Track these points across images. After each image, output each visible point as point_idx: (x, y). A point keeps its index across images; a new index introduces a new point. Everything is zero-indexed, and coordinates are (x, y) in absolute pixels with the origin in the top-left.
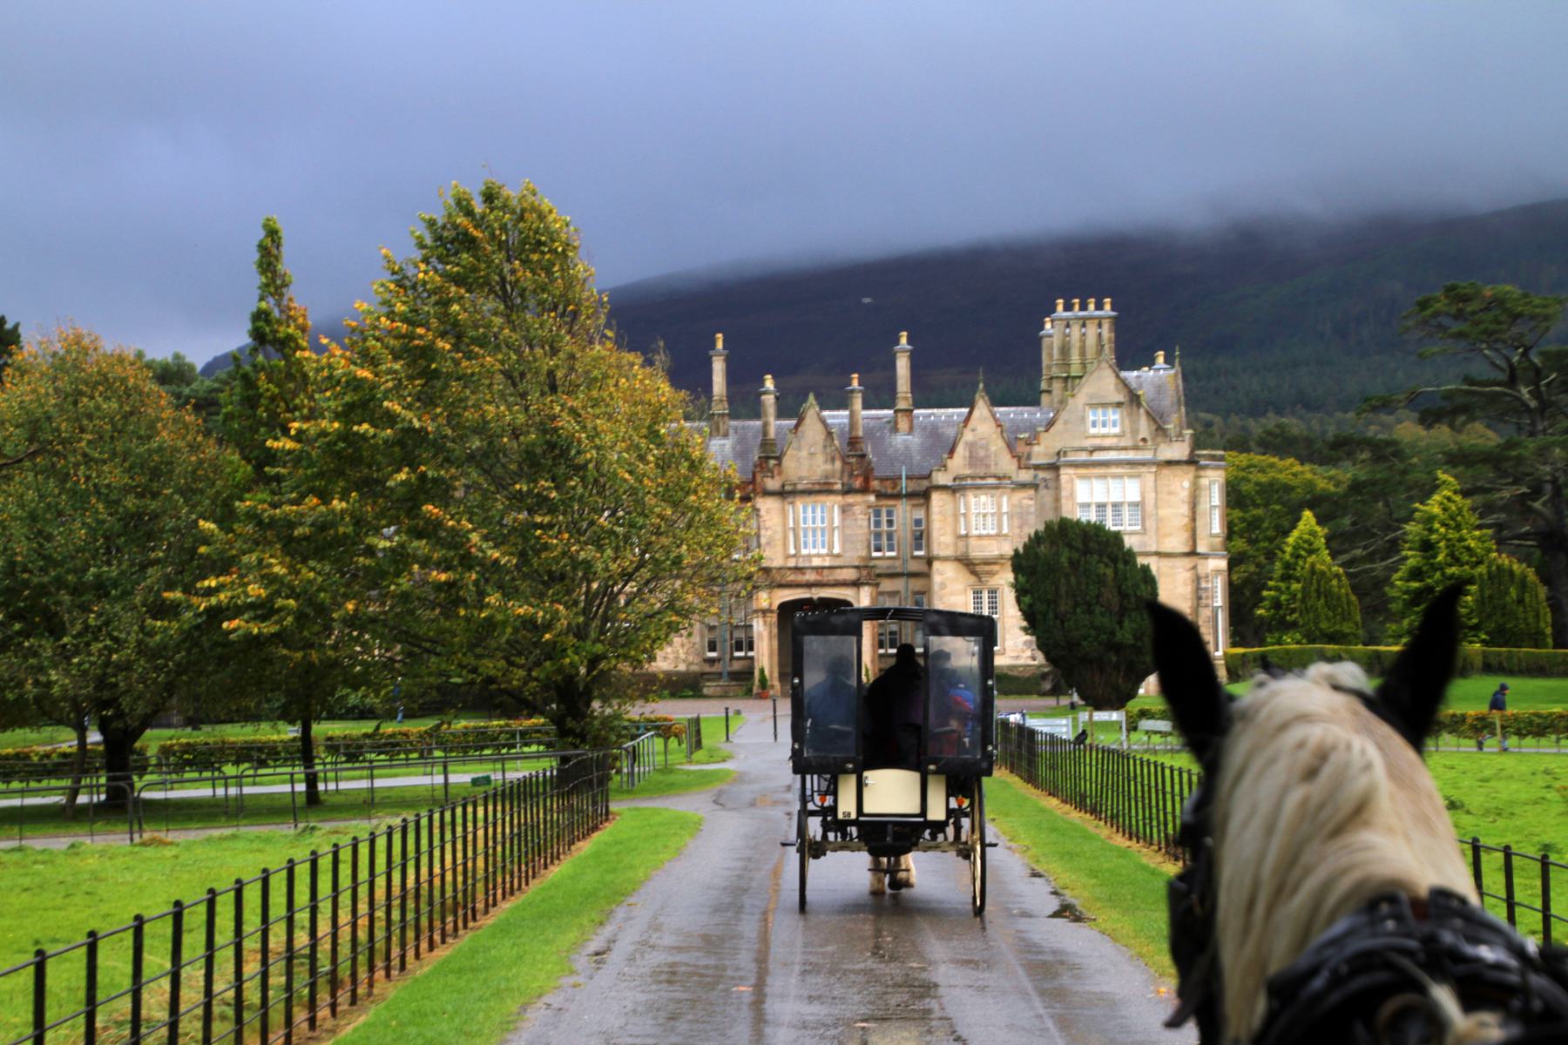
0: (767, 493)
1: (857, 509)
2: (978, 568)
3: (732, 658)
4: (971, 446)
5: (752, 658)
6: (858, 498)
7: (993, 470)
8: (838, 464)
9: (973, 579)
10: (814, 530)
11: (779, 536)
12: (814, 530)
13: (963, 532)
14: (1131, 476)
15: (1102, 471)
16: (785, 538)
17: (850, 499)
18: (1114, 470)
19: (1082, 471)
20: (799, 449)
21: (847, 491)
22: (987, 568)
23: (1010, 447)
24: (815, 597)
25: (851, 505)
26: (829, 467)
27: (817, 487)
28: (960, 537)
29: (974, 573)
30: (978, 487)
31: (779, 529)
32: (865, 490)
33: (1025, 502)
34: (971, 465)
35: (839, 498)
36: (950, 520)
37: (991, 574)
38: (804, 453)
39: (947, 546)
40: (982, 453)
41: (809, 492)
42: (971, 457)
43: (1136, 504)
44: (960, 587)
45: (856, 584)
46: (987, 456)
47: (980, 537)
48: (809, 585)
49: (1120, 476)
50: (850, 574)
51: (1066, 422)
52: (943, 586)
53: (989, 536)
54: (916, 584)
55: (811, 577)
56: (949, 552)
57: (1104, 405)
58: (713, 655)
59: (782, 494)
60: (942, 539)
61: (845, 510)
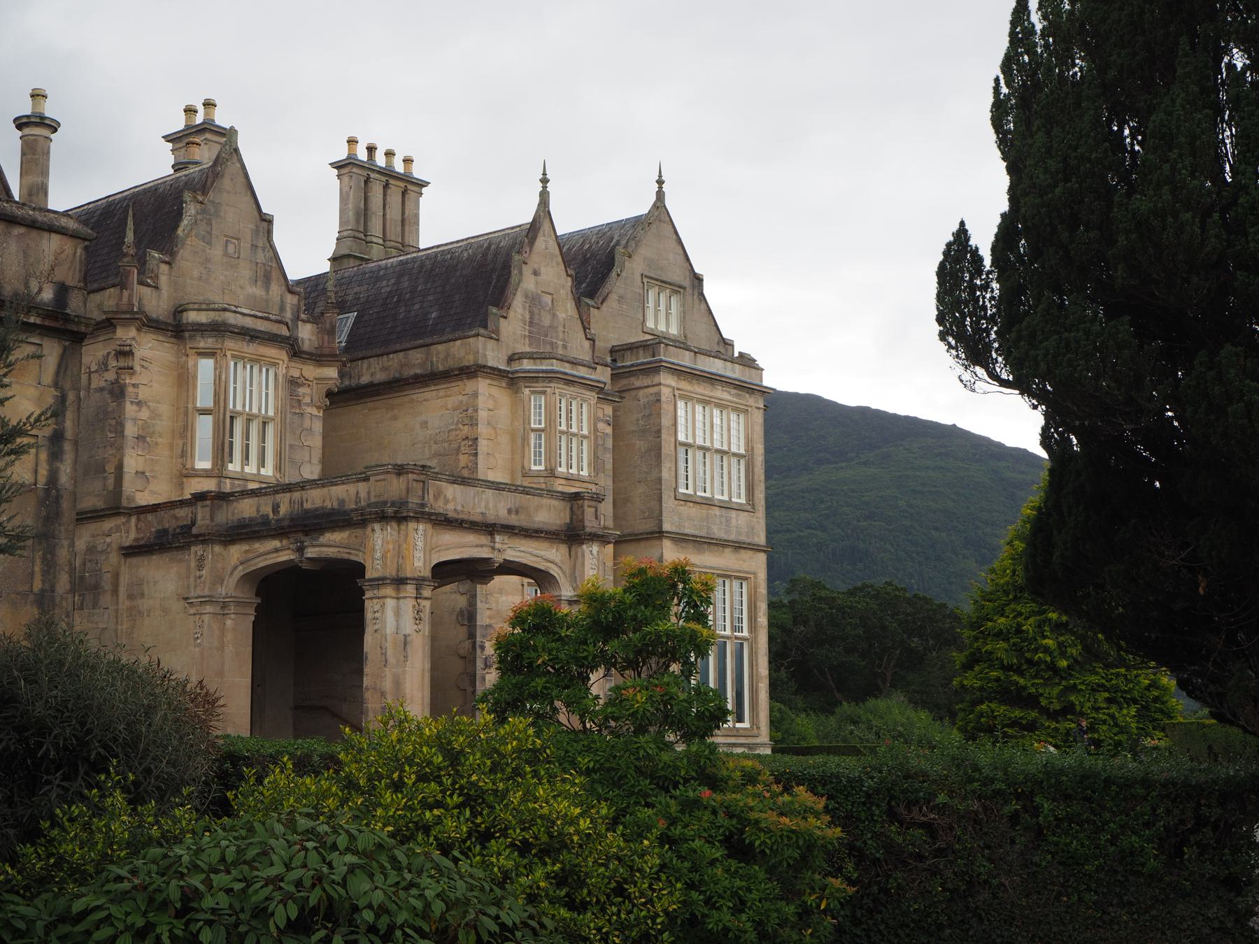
7: (560, 351)
8: (276, 289)
11: (164, 425)
15: (702, 389)
16: (185, 432)
18: (721, 393)
19: (684, 385)
20: (208, 240)
26: (258, 291)
27: (261, 326)
30: (569, 381)
31: (165, 409)
34: (531, 338)
38: (216, 252)
42: (531, 323)
46: (553, 327)
48: (489, 528)
49: (722, 406)
51: (621, 298)
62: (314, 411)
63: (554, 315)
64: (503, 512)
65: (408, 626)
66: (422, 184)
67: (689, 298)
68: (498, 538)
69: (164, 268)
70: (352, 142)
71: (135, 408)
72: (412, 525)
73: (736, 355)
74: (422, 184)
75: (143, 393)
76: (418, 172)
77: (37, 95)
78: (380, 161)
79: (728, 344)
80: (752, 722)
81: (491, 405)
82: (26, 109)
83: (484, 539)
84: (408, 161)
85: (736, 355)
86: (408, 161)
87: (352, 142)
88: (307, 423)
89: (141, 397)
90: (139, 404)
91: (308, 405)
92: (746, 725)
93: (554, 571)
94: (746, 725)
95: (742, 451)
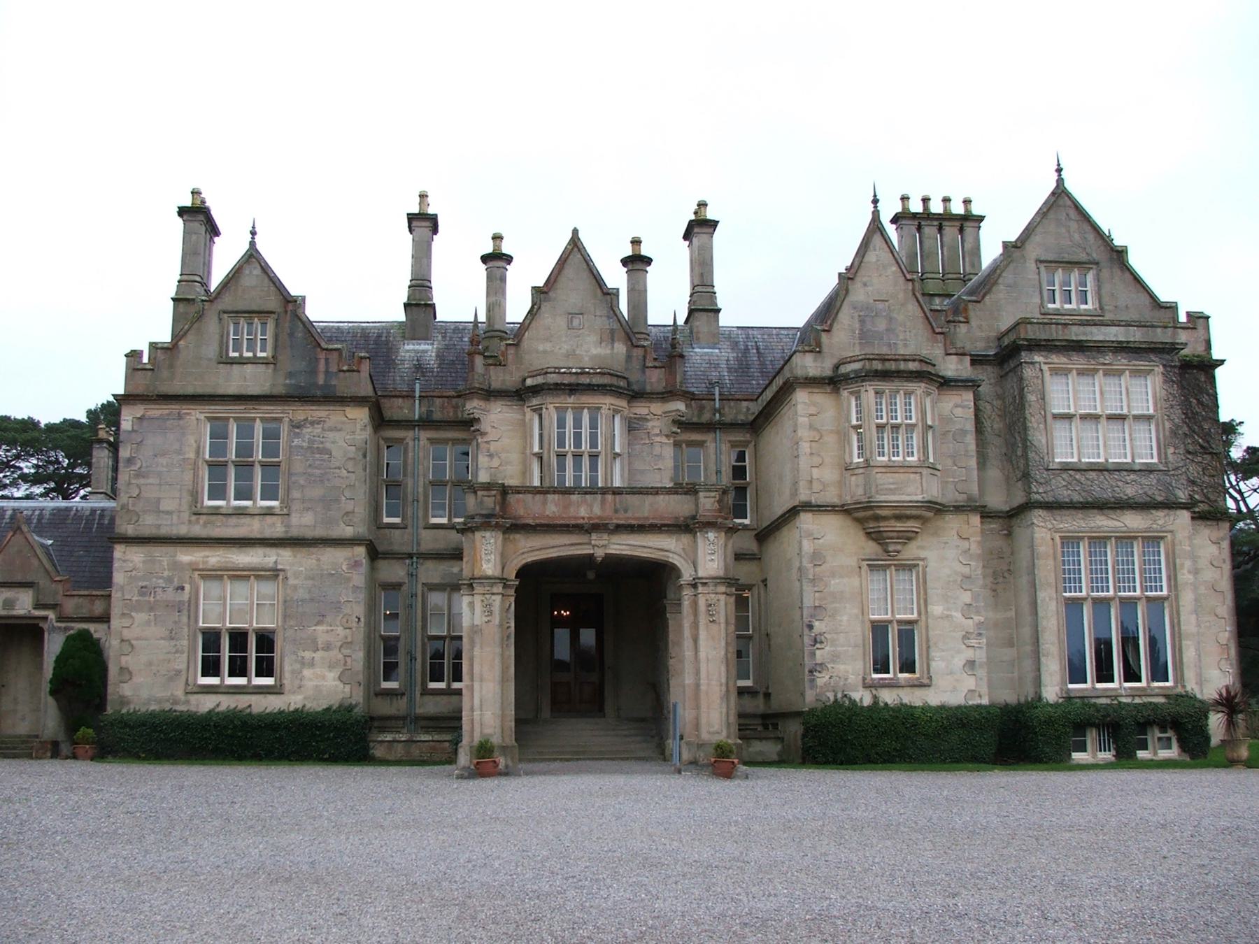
0: (491, 394)
1: (655, 426)
2: (884, 526)
3: (426, 692)
4: (866, 314)
5: (459, 692)
6: (657, 408)
8: (621, 348)
9: (871, 548)
10: (577, 457)
12: (577, 457)
13: (856, 460)
14: (1136, 373)
17: (641, 409)
21: (635, 395)
22: (899, 526)
23: (930, 318)
24: (600, 553)
25: (643, 419)
28: (848, 468)
29: (876, 536)
31: (515, 457)
32: (667, 395)
33: (959, 411)
35: (623, 403)
36: (831, 440)
37: (908, 537)
39: (825, 486)
40: (881, 325)
41: (573, 389)
43: (1148, 418)
44: (852, 562)
45: (688, 527)
47: (890, 467)
50: (678, 506)
52: (817, 558)
53: (904, 467)
54: (745, 572)
55: (585, 510)
56: (831, 496)
57: (1071, 264)
58: (393, 685)
59: (520, 394)
60: (816, 473)
61: (633, 426)
62: (664, 440)
63: (891, 320)
64: (609, 512)
65: (479, 619)
66: (981, 219)
67: (1105, 273)
68: (594, 536)
69: (511, 351)
70: (904, 199)
71: (486, 459)
72: (478, 535)
73: (1183, 318)
74: (981, 219)
75: (493, 447)
76: (976, 210)
77: (497, 238)
78: (936, 207)
79: (1172, 308)
80: (1176, 682)
81: (813, 410)
82: (489, 249)
83: (584, 539)
84: (967, 202)
85: (1183, 318)
86: (967, 202)
87: (904, 199)
88: (657, 450)
89: (492, 449)
90: (491, 456)
91: (657, 435)
92: (1170, 684)
93: (676, 560)
94: (1170, 684)
95: (1151, 411)
